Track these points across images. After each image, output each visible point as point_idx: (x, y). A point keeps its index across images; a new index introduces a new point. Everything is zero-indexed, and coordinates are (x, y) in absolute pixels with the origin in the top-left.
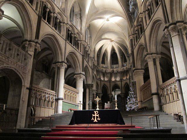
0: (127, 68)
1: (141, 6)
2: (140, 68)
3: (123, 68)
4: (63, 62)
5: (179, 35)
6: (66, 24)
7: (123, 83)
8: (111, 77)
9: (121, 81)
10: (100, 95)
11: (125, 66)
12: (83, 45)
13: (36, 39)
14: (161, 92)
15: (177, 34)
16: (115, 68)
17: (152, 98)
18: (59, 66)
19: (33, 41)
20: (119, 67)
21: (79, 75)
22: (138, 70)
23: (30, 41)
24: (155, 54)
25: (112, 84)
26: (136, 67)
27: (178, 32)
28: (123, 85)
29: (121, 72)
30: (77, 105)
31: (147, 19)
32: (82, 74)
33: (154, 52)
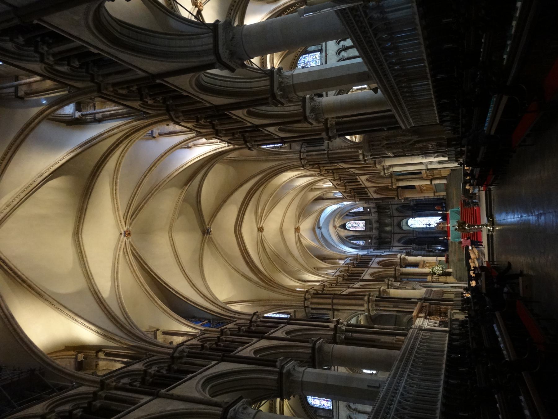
0: (373, 208)
1: (337, 188)
2: (396, 192)
3: (374, 213)
4: (395, 269)
5: (393, 167)
6: (349, 268)
7: (396, 213)
8: (385, 231)
9: (393, 217)
10: (415, 248)
11: (370, 210)
12: (362, 257)
13: (385, 281)
14: (431, 177)
15: (391, 168)
16: (371, 226)
17: (435, 184)
18: (399, 274)
19: (389, 282)
20: (370, 219)
21: (402, 261)
22: (399, 195)
23: (388, 285)
24: (392, 180)
25: (397, 230)
26: (394, 196)
27: (391, 167)
28: (400, 215)
29: (378, 216)
30: (438, 262)
31: (353, 184)
32: (401, 257)
33: (390, 180)
